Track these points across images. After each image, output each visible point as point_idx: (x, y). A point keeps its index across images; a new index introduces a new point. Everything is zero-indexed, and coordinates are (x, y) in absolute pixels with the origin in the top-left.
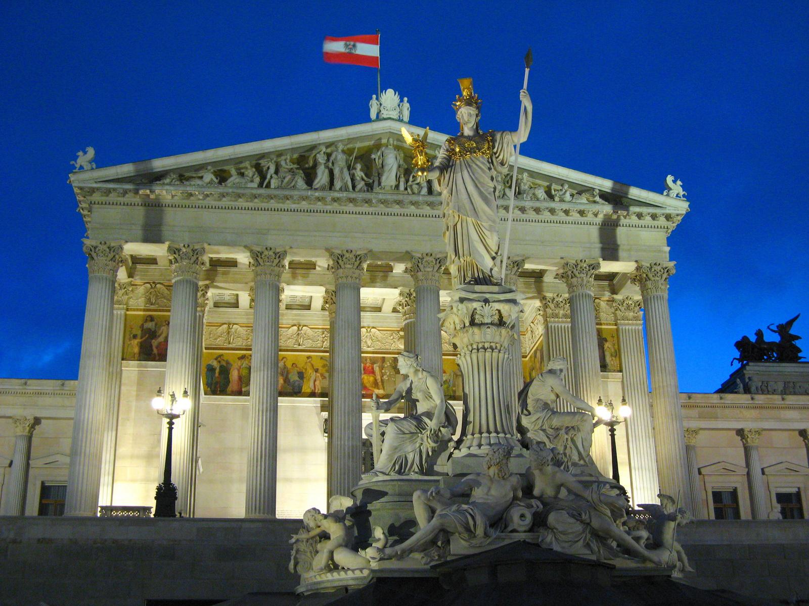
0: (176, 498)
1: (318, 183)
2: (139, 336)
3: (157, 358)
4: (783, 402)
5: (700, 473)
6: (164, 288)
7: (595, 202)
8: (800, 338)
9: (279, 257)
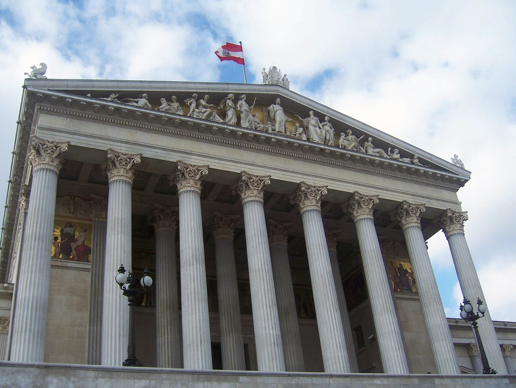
2: (59, 240)
3: (76, 258)
9: (202, 173)
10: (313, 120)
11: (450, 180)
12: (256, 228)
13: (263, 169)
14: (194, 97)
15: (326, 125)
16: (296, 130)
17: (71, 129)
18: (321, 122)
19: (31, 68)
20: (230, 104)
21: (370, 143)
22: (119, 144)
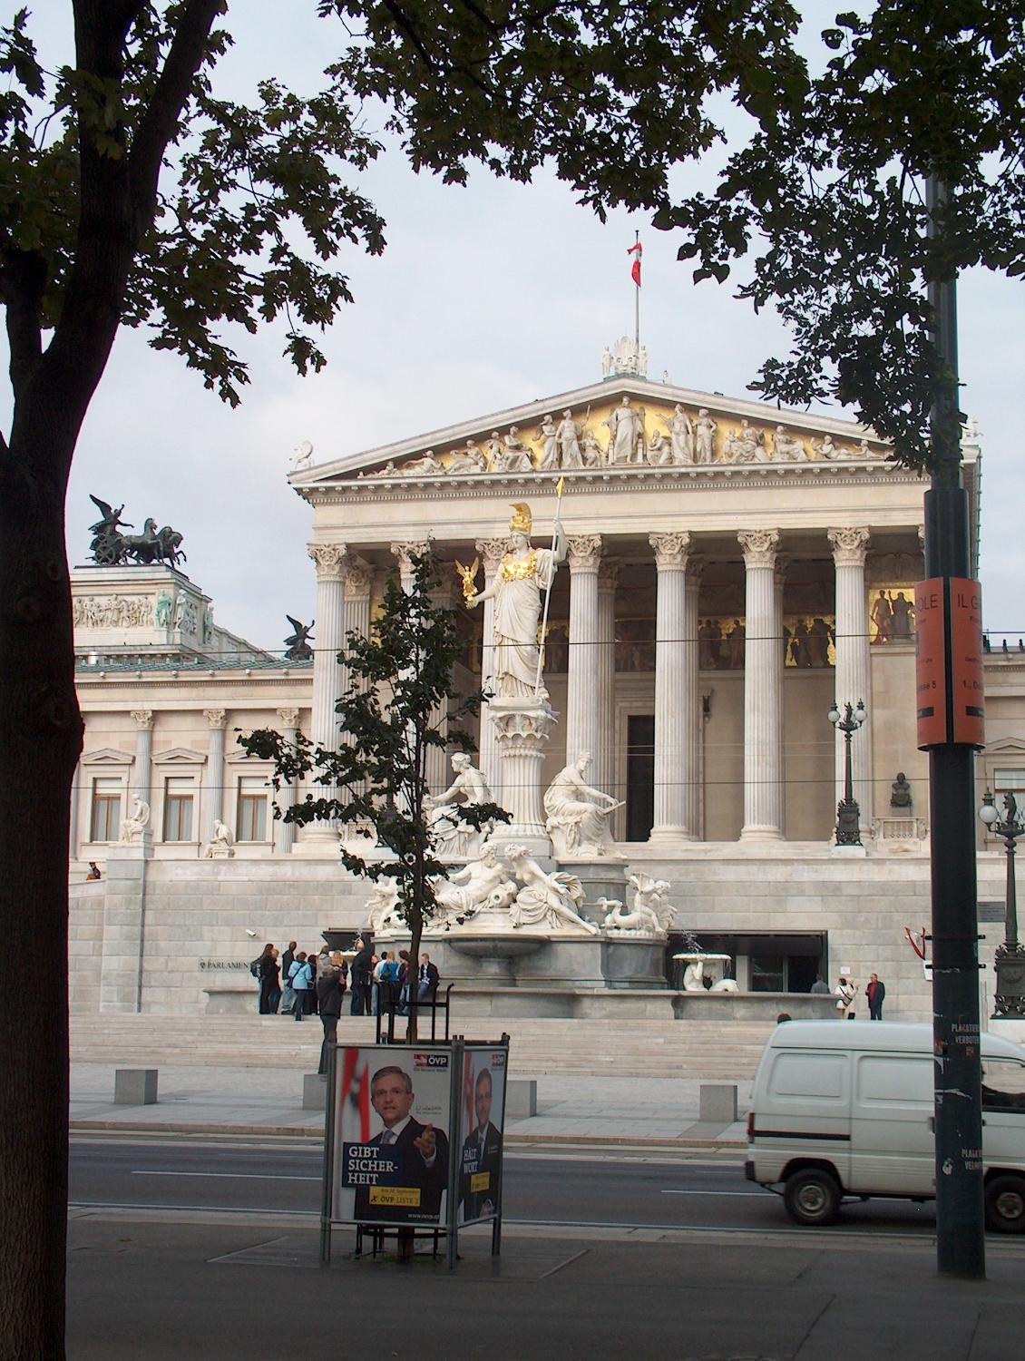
10: (680, 417)
13: (595, 522)
14: (495, 438)
17: (349, 522)
18: (691, 421)
21: (781, 437)
22: (407, 528)
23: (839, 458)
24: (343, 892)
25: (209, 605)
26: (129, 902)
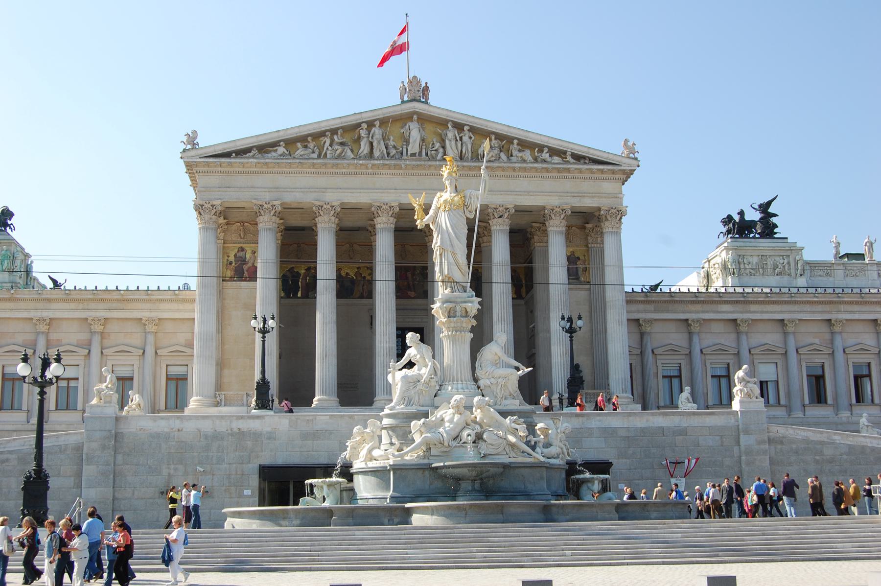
0: (270, 389)
1: (362, 152)
4: (720, 299)
5: (652, 350)
6: (250, 225)
7: (568, 161)
8: (778, 216)
9: (335, 209)
10: (451, 133)
11: (613, 172)
12: (382, 255)
15: (465, 136)
16: (433, 144)
18: (459, 134)
19: (185, 135)
20: (363, 135)
21: (515, 146)
23: (553, 162)
24: (269, 438)
25: (30, 260)
26: (104, 448)
